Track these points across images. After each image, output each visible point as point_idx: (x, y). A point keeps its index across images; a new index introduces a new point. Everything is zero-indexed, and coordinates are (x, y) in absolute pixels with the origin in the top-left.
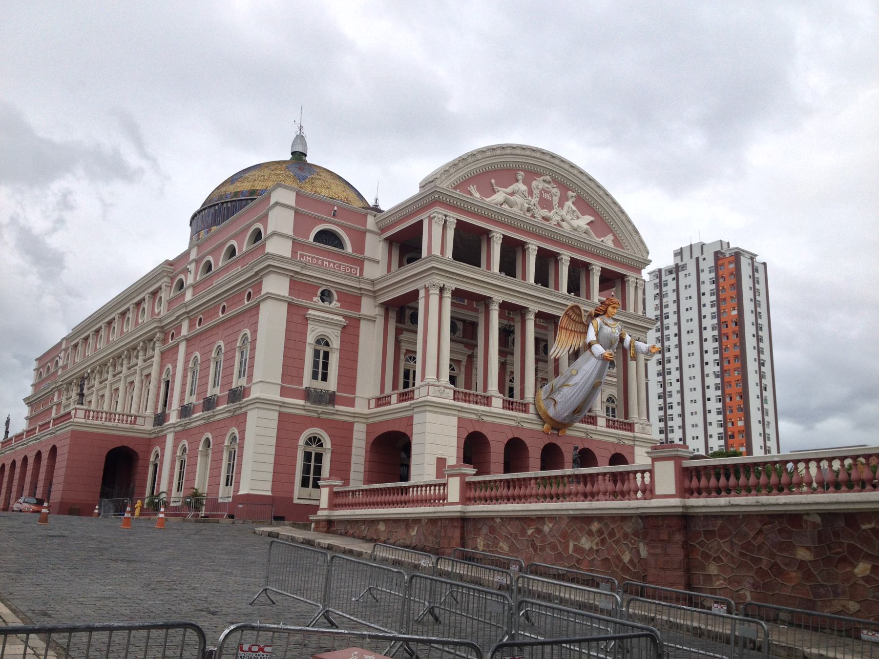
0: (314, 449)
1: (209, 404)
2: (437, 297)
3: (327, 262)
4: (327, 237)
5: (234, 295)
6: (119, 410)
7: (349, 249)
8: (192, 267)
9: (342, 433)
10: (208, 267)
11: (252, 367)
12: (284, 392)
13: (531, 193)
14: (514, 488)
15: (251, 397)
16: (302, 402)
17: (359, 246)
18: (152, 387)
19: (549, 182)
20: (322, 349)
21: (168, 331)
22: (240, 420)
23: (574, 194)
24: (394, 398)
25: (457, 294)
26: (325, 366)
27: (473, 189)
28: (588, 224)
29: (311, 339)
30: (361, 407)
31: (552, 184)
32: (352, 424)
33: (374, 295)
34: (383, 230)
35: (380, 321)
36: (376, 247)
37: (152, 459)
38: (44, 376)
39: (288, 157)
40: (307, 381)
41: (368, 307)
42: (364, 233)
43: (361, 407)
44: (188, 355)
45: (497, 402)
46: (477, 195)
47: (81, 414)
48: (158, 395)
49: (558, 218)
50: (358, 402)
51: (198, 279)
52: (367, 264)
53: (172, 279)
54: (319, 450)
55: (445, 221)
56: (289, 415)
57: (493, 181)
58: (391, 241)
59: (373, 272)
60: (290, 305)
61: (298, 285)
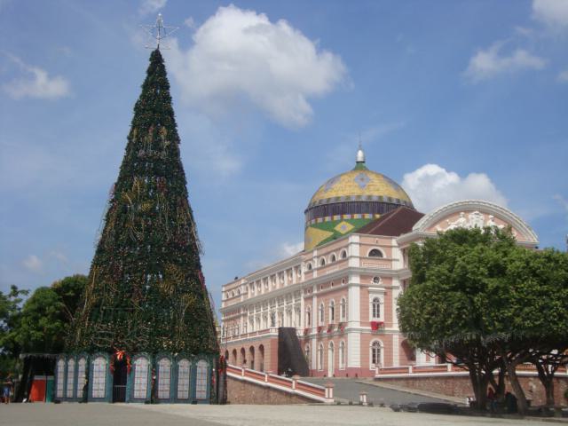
0: (376, 347)
5: (337, 281)
12: (362, 323)
17: (389, 254)
21: (308, 289)
26: (378, 311)
40: (371, 319)
44: (318, 302)
51: (320, 266)
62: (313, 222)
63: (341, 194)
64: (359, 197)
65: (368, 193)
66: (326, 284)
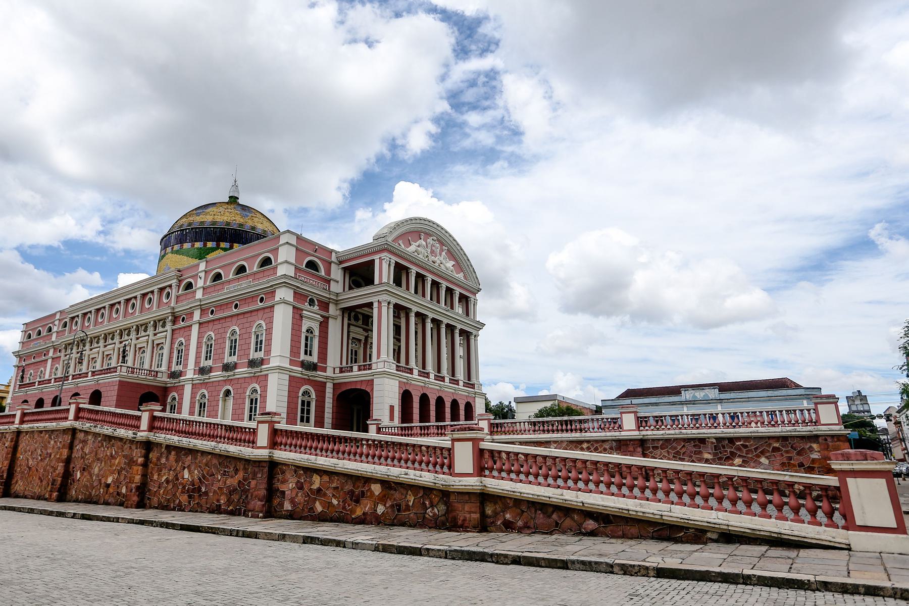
0: (306, 399)
1: (227, 367)
3: (313, 281)
4: (312, 265)
5: (250, 298)
6: (147, 366)
7: (323, 273)
8: (202, 275)
9: (320, 387)
10: (218, 277)
11: (269, 345)
12: (292, 362)
15: (270, 365)
16: (300, 369)
17: (328, 272)
18: (166, 351)
20: (310, 335)
22: (263, 380)
24: (355, 368)
27: (400, 242)
29: (304, 329)
30: (329, 373)
32: (325, 383)
33: (337, 303)
34: (341, 262)
35: (340, 319)
36: (337, 273)
37: (169, 400)
38: (34, 336)
39: (227, 200)
40: (303, 357)
41: (333, 310)
42: (330, 263)
43: (329, 373)
45: (416, 372)
47: (124, 369)
48: (170, 358)
50: (328, 369)
52: (332, 283)
53: (180, 281)
54: (309, 399)
56: (294, 377)
58: (345, 269)
59: (336, 288)
60: (294, 307)
61: (299, 295)
62: (176, 247)
63: (219, 219)
64: (241, 225)
65: (250, 223)
66: (222, 305)
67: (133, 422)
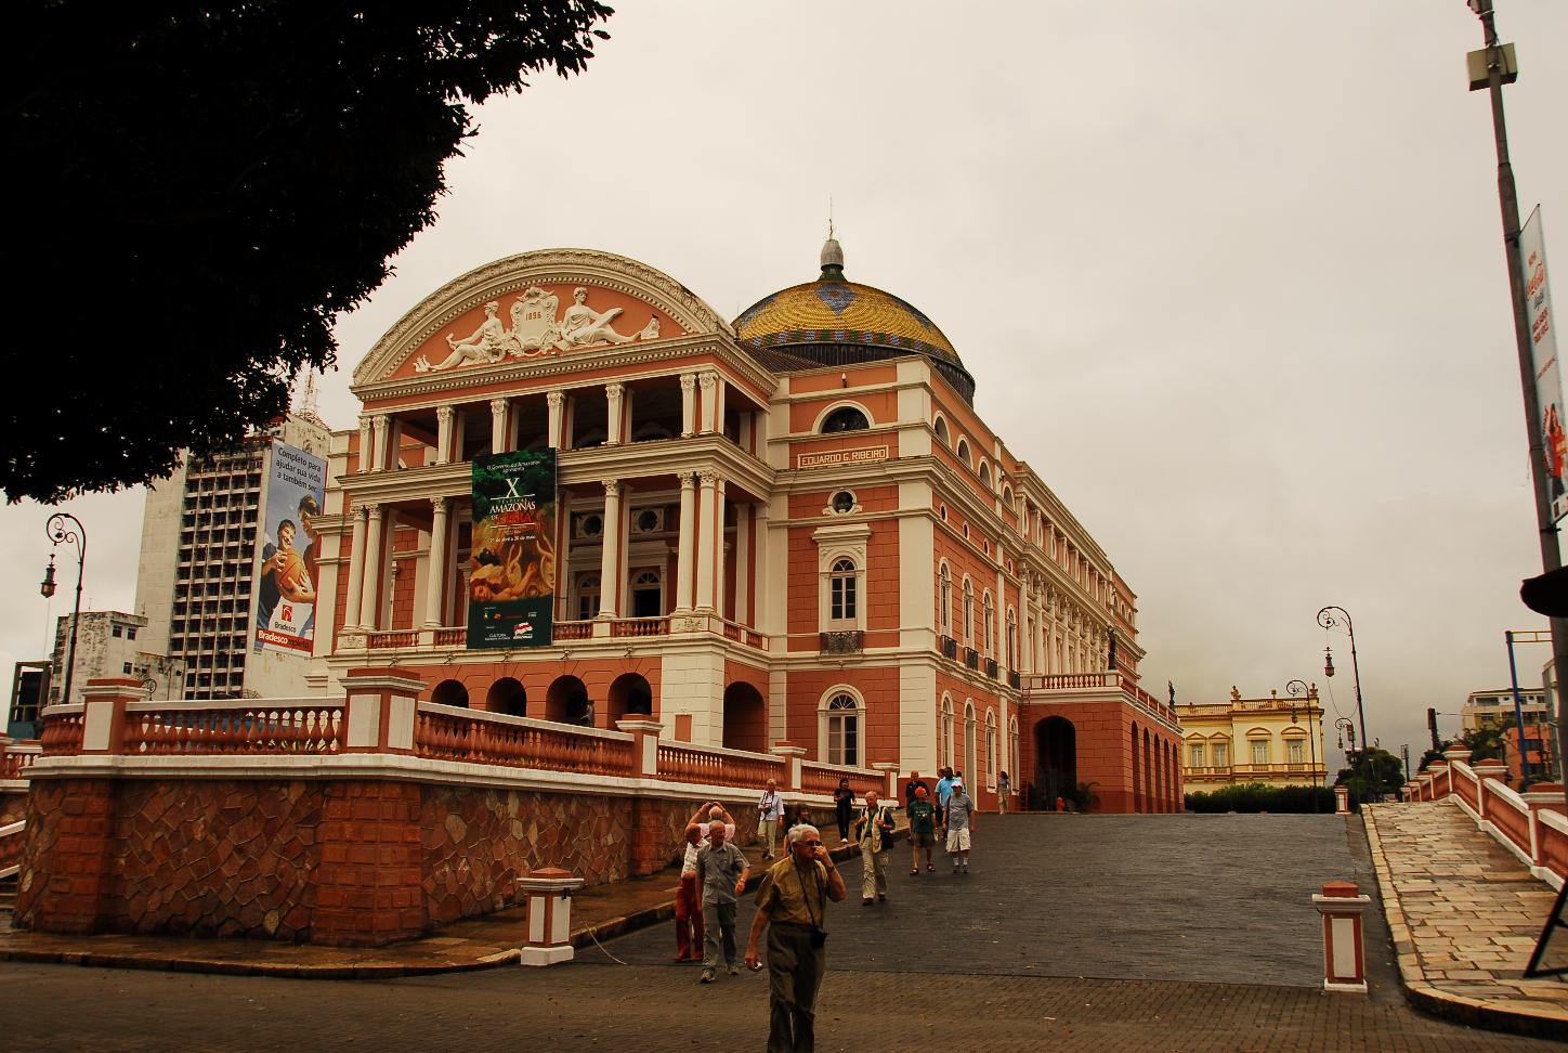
2: (362, 524)
13: (507, 324)
14: (574, 747)
19: (537, 294)
23: (581, 289)
25: (385, 509)
28: (613, 321)
31: (542, 292)
46: (428, 365)
49: (553, 339)
55: (372, 423)
57: (449, 338)
67: (811, 780)
